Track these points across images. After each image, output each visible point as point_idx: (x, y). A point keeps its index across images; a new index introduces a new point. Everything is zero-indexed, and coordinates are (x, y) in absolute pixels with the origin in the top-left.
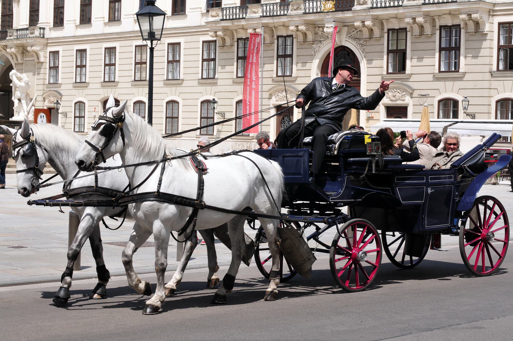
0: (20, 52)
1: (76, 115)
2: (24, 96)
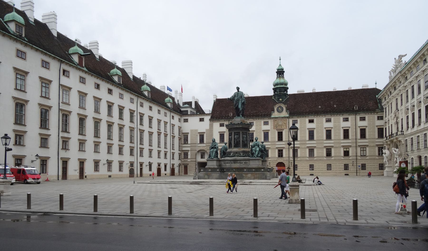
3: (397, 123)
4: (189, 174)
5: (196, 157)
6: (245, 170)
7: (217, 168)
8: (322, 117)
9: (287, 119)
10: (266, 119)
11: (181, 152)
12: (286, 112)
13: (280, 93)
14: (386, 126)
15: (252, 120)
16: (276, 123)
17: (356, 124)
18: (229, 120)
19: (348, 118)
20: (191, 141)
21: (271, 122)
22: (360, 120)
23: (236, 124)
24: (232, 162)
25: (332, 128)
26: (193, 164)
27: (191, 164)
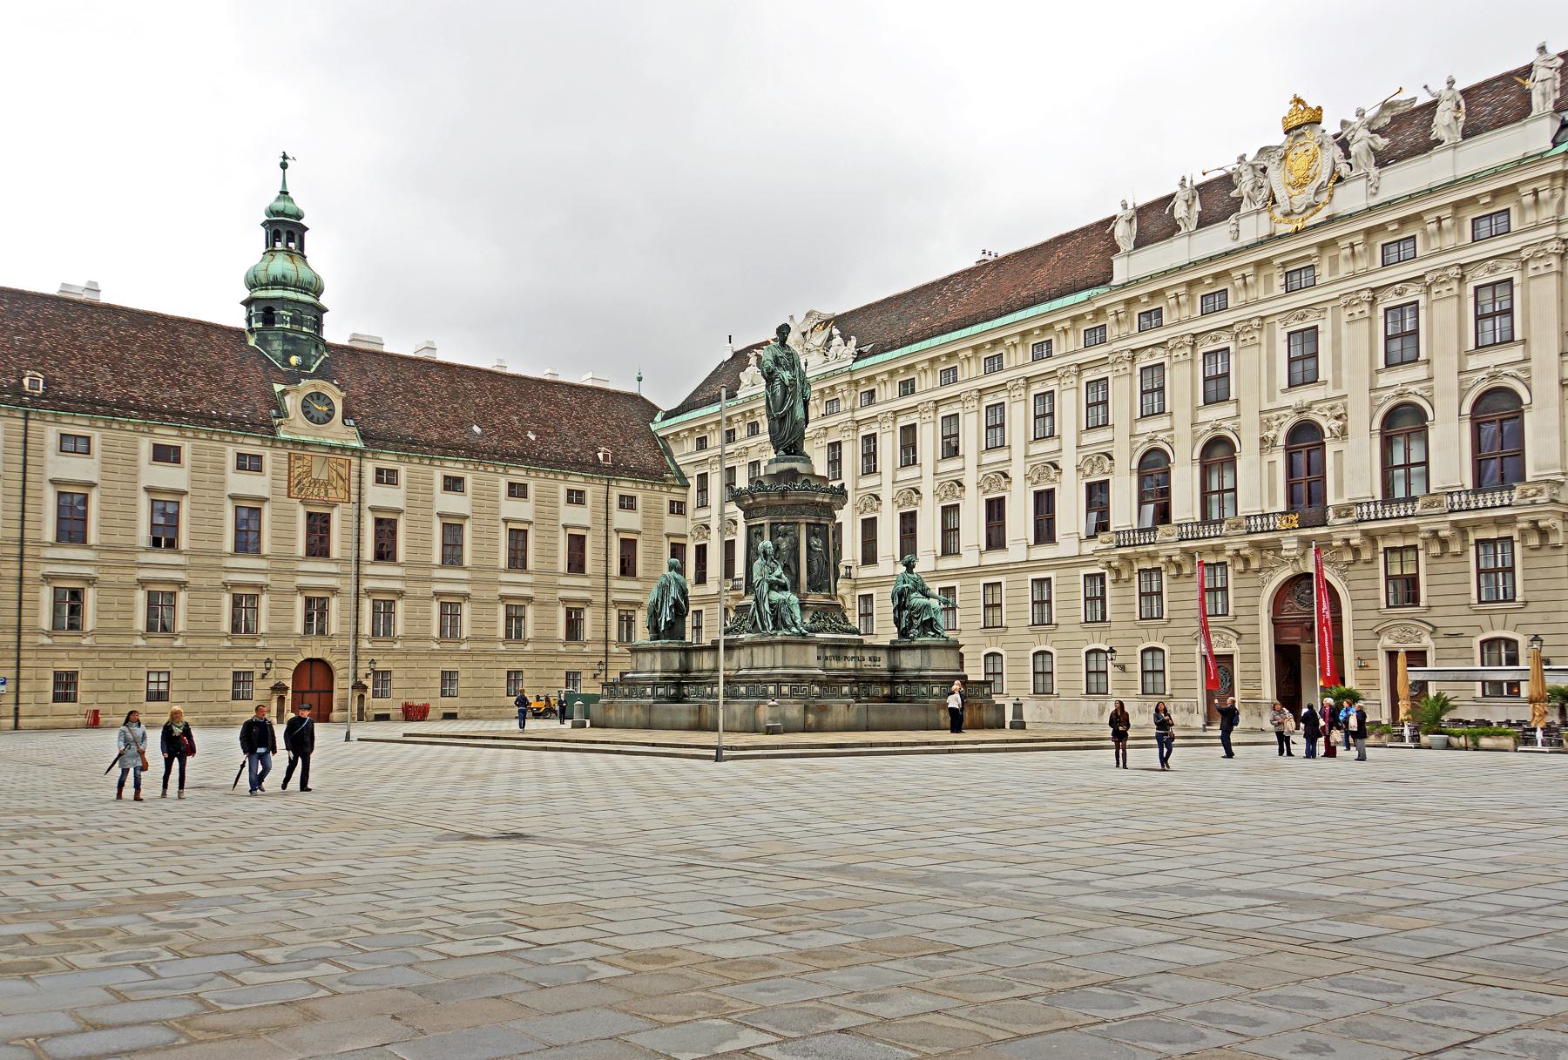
8: (495, 472)
9: (355, 461)
10: (247, 441)
15: (174, 433)
16: (300, 470)
18: (27, 413)
19: (581, 493)
21: (274, 461)
22: (622, 506)
24: (828, 653)
25: (530, 523)
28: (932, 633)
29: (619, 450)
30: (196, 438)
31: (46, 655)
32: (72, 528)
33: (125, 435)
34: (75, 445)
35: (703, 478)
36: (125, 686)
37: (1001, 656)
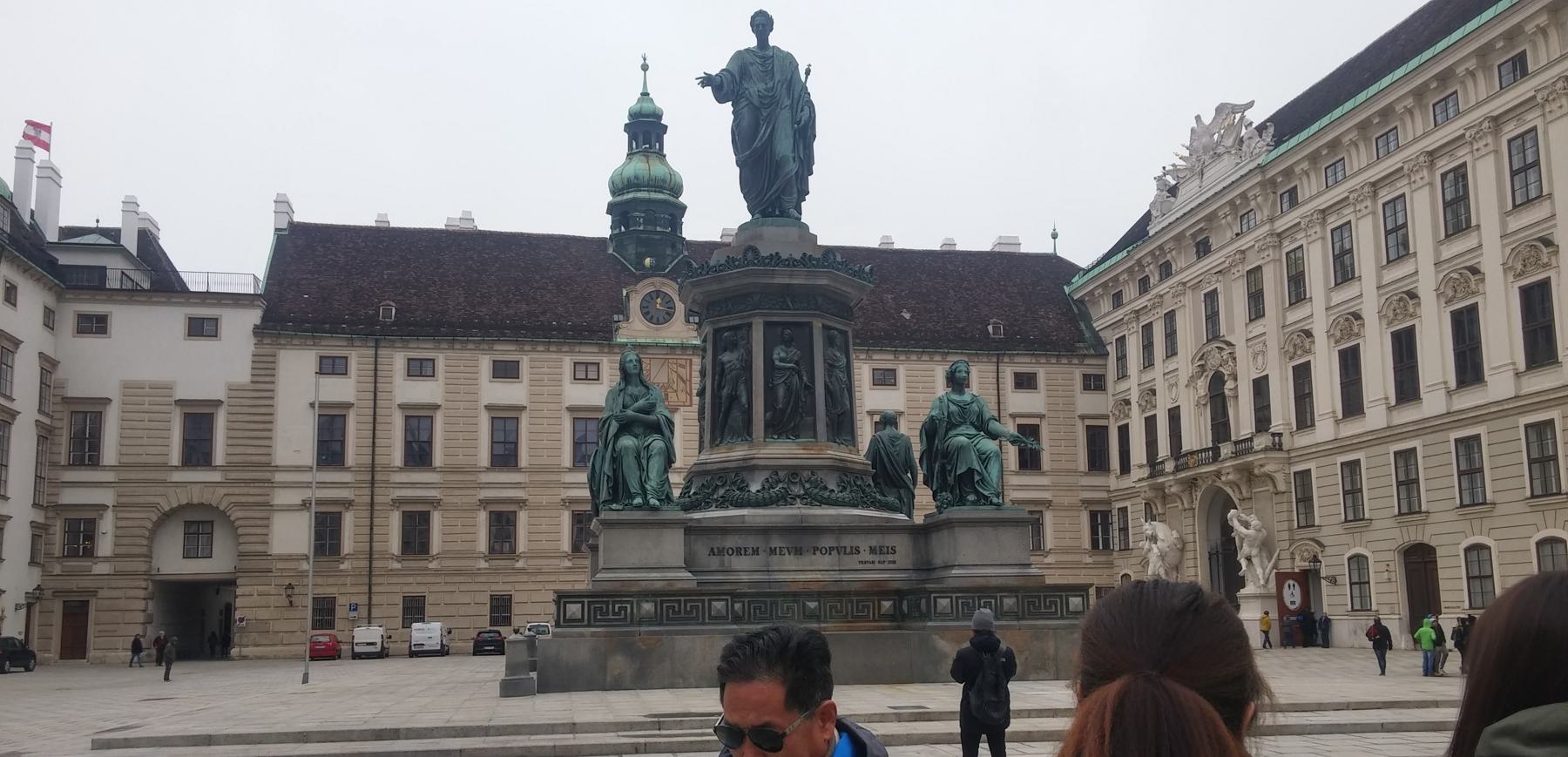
0: (1245, 479)
1: (1353, 581)
2: (1254, 552)
3: (1218, 400)
4: (99, 654)
5: (151, 552)
6: (944, 603)
7: (693, 585)
11: (46, 518)
12: (688, 321)
13: (650, 228)
14: (1127, 416)
17: (999, 403)
18: (377, 341)
20: (125, 450)
23: (792, 263)
24: (776, 542)
26: (131, 593)
27: (115, 593)
28: (971, 497)
29: (1017, 320)
30: (534, 350)
31: (395, 580)
32: (418, 454)
33: (466, 354)
34: (419, 369)
35: (1121, 341)
36: (471, 610)
37: (1489, 548)
